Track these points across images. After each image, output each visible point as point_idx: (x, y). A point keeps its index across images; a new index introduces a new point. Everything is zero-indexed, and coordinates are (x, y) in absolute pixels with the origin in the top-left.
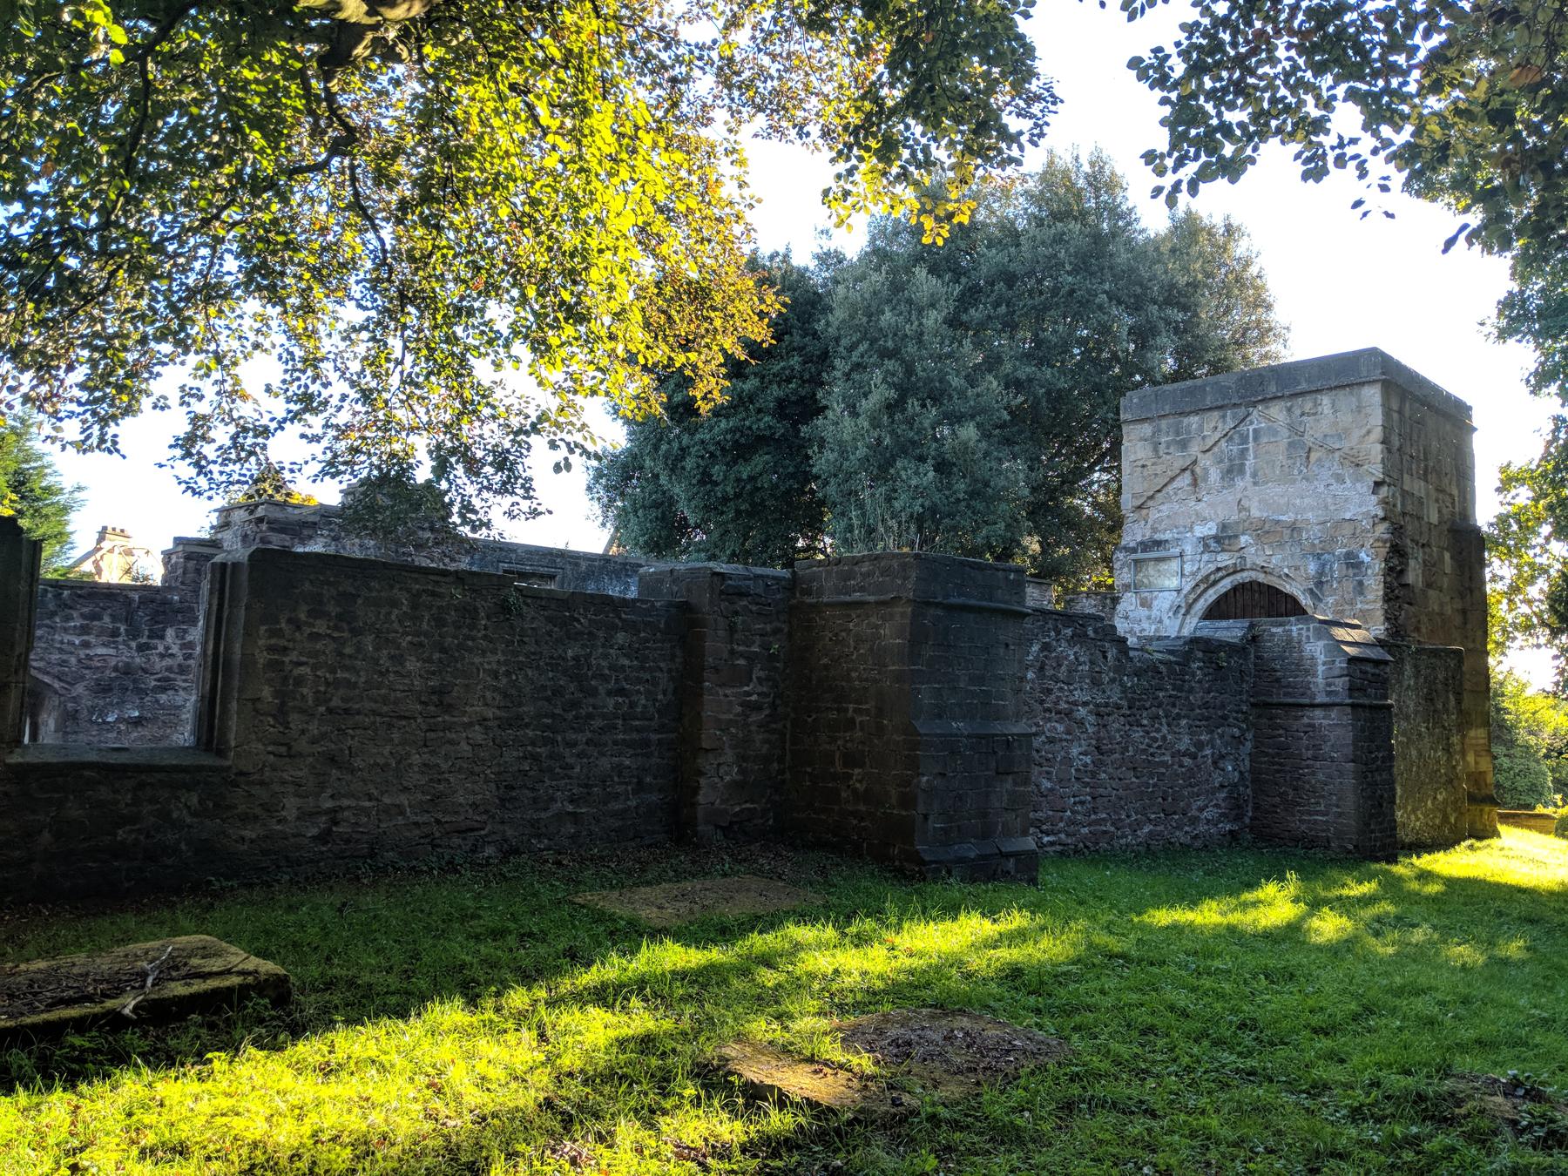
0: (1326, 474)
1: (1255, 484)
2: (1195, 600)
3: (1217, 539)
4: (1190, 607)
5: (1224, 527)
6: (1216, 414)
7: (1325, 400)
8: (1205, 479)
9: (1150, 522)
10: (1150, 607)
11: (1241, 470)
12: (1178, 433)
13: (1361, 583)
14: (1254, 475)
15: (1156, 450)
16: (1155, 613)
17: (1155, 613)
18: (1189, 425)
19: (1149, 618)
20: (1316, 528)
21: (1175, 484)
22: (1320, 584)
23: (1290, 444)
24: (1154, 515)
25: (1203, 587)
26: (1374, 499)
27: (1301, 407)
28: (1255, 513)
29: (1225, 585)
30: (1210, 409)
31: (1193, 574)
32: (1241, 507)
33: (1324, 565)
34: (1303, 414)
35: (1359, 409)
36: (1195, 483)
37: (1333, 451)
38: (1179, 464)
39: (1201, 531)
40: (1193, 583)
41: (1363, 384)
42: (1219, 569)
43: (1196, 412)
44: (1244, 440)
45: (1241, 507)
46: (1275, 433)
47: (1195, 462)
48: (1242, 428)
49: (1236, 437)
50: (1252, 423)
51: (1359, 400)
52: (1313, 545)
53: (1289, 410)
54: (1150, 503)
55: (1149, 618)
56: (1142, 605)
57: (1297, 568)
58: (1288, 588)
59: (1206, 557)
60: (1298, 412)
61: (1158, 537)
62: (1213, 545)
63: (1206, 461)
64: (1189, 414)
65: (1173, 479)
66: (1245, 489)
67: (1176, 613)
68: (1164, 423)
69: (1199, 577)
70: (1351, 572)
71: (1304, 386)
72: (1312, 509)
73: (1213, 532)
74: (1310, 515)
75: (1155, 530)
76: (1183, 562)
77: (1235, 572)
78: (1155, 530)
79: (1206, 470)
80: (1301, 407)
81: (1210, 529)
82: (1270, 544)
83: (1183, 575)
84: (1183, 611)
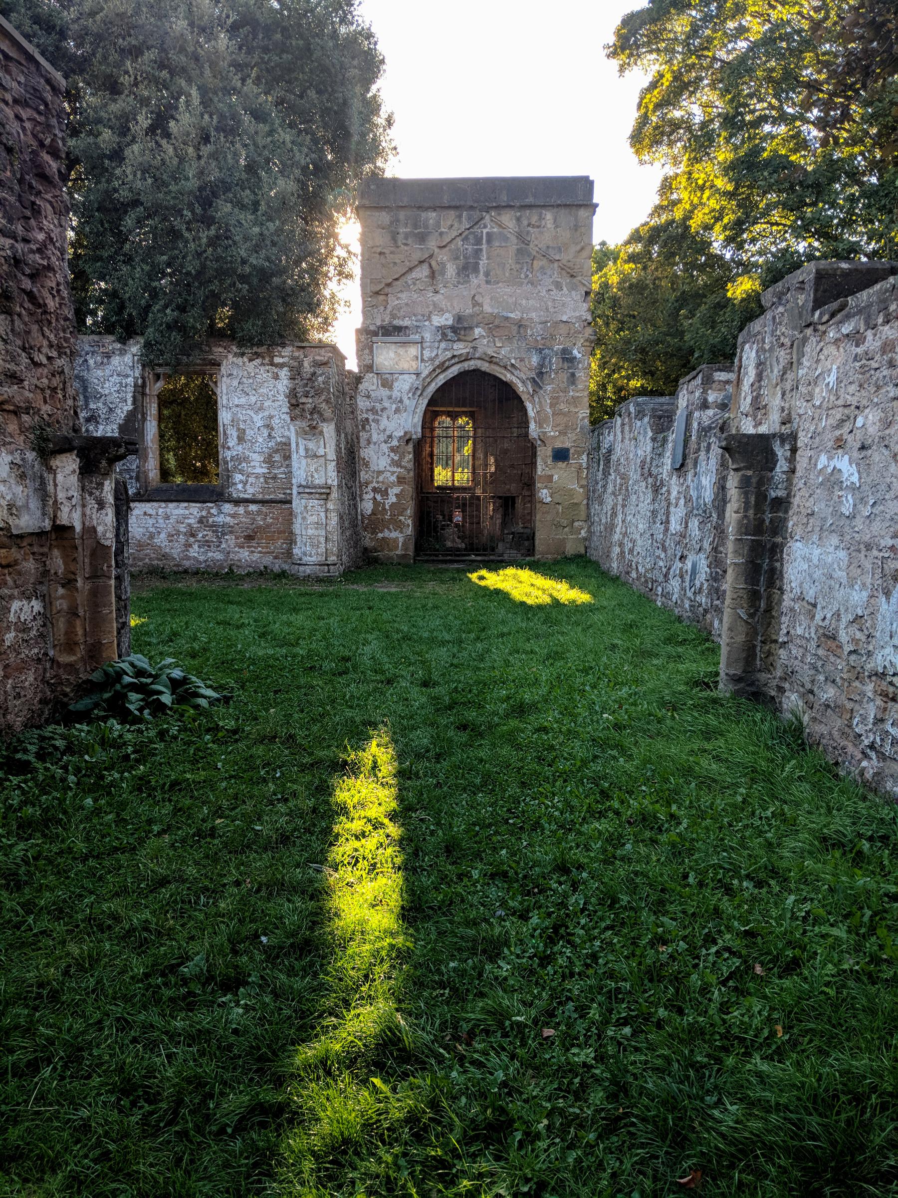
0: (547, 281)
1: (488, 282)
2: (429, 384)
3: (454, 329)
4: (424, 388)
5: (459, 318)
6: (452, 213)
7: (549, 216)
8: (443, 272)
9: (389, 308)
10: (391, 388)
11: (476, 269)
12: (416, 226)
13: (573, 375)
14: (487, 274)
15: (394, 239)
16: (396, 394)
17: (396, 394)
18: (427, 219)
19: (390, 397)
20: (539, 327)
21: (414, 275)
22: (541, 374)
23: (518, 250)
24: (393, 302)
25: (438, 371)
26: (585, 306)
27: (529, 219)
28: (487, 309)
29: (454, 371)
30: (449, 207)
31: (432, 360)
32: (476, 304)
33: (544, 359)
34: (529, 225)
35: (576, 228)
36: (433, 275)
37: (551, 261)
38: (417, 256)
39: (438, 320)
40: (431, 368)
41: (580, 206)
42: (454, 356)
43: (434, 209)
44: (478, 241)
45: (476, 304)
46: (506, 239)
47: (431, 256)
48: (475, 229)
49: (471, 237)
50: (485, 227)
51: (576, 219)
53: (518, 219)
54: (389, 290)
55: (390, 397)
56: (383, 386)
57: (522, 360)
58: (508, 377)
59: (443, 345)
60: (525, 223)
61: (397, 322)
62: (450, 335)
63: (443, 256)
64: (427, 209)
65: (411, 269)
66: (479, 286)
67: (414, 394)
68: (402, 215)
69: (437, 363)
70: (566, 365)
71: (530, 200)
72: (535, 310)
73: (450, 322)
74: (533, 315)
75: (394, 316)
77: (466, 360)
78: (394, 316)
79: (443, 265)
80: (529, 219)
81: (446, 320)
82: (500, 337)
83: (422, 360)
84: (419, 392)
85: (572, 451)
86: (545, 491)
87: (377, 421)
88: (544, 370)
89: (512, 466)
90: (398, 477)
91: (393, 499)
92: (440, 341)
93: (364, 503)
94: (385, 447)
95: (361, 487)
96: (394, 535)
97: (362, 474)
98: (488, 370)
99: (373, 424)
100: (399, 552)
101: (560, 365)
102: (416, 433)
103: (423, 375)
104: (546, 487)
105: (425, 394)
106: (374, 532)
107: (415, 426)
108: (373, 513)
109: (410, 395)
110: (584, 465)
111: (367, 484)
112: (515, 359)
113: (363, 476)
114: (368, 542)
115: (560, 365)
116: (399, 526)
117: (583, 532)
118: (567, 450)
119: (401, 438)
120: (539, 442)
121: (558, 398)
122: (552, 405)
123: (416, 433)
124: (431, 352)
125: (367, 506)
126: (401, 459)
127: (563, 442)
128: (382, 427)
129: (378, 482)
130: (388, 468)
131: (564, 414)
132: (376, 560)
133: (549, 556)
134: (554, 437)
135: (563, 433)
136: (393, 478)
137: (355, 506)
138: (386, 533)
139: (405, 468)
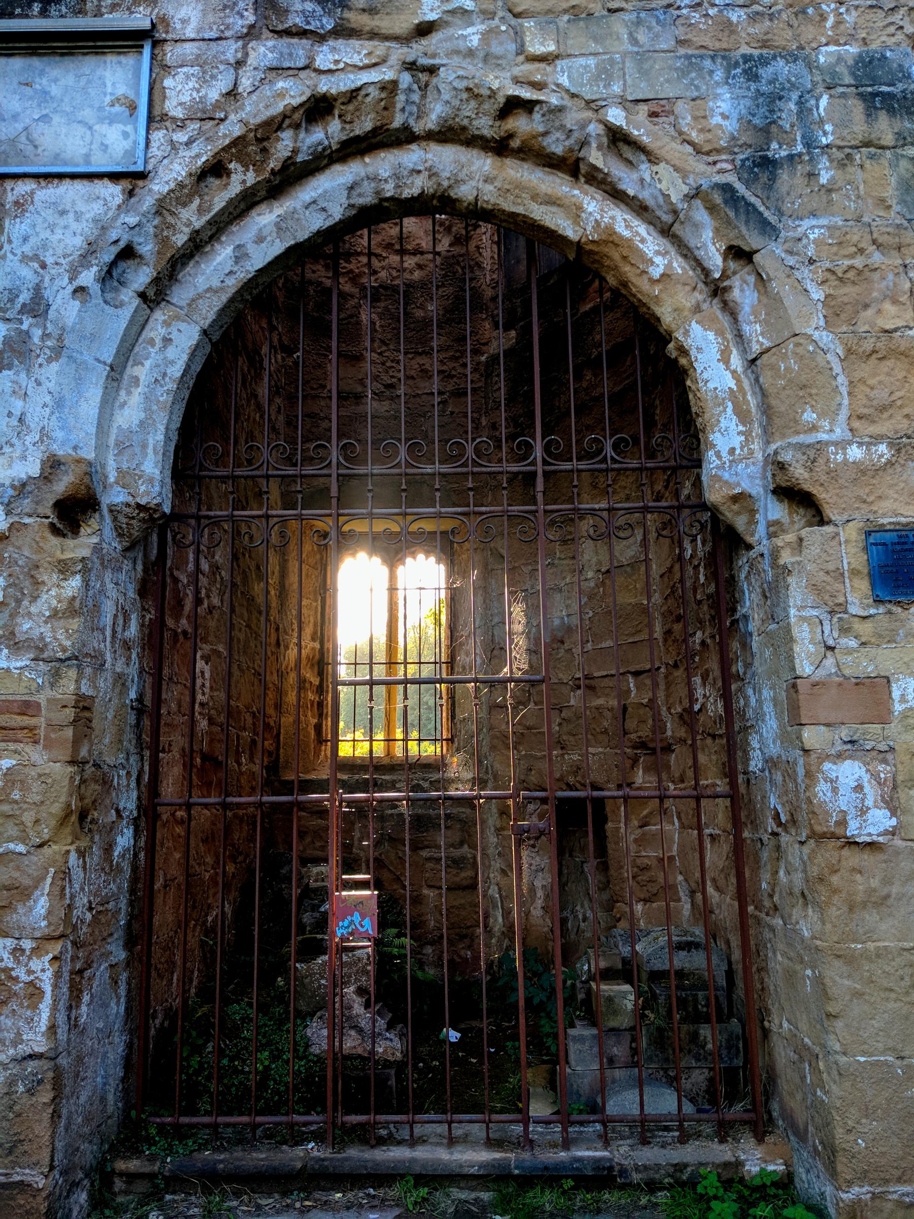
33: (774, 98)
40: (203, 153)
52: (729, 27)
69: (232, 129)
76: (159, 67)
83: (155, 119)
88: (776, 151)
89: (589, 685)
92: (250, 34)
98: (490, 196)
101: (859, 128)
102: (126, 478)
103: (159, 186)
105: (180, 295)
109: (88, 277)
112: (630, 104)
115: (859, 128)
119: (21, 488)
120: (776, 510)
121: (863, 274)
123: (126, 478)
124: (204, 80)
134: (862, 471)
139: (39, 651)
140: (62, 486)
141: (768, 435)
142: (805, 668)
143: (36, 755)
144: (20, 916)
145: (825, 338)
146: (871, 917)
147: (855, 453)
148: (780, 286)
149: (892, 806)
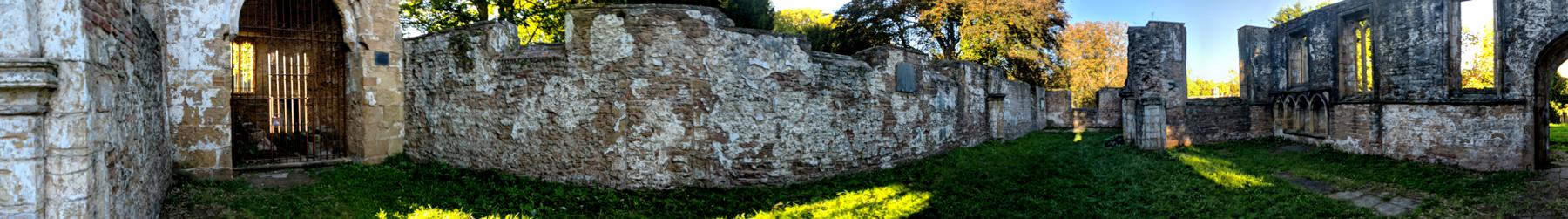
85: (390, 56)
86: (370, 94)
87: (188, 13)
90: (214, 77)
91: (207, 104)
93: (172, 109)
94: (197, 42)
95: (168, 89)
96: (210, 147)
97: (170, 74)
99: (183, 16)
100: (216, 167)
104: (371, 90)
106: (185, 145)
107: (232, 21)
108: (184, 122)
110: (401, 70)
111: (176, 86)
113: (172, 76)
114: (178, 156)
116: (216, 136)
117: (401, 132)
118: (387, 55)
119: (217, 31)
120: (359, 46)
121: (376, 7)
122: (372, 13)
125: (176, 113)
126: (216, 56)
127: (383, 48)
128: (194, 19)
129: (189, 84)
130: (202, 66)
131: (382, 23)
132: (188, 177)
133: (376, 157)
134: (375, 42)
135: (383, 39)
136: (208, 79)
137: (160, 116)
138: (200, 146)
140: (225, 31)
141: (358, 32)
142: (365, 75)
143: (224, 88)
144: (222, 121)
145: (370, 16)
146: (371, 117)
147: (374, 38)
148: (364, 7)
149: (376, 99)
